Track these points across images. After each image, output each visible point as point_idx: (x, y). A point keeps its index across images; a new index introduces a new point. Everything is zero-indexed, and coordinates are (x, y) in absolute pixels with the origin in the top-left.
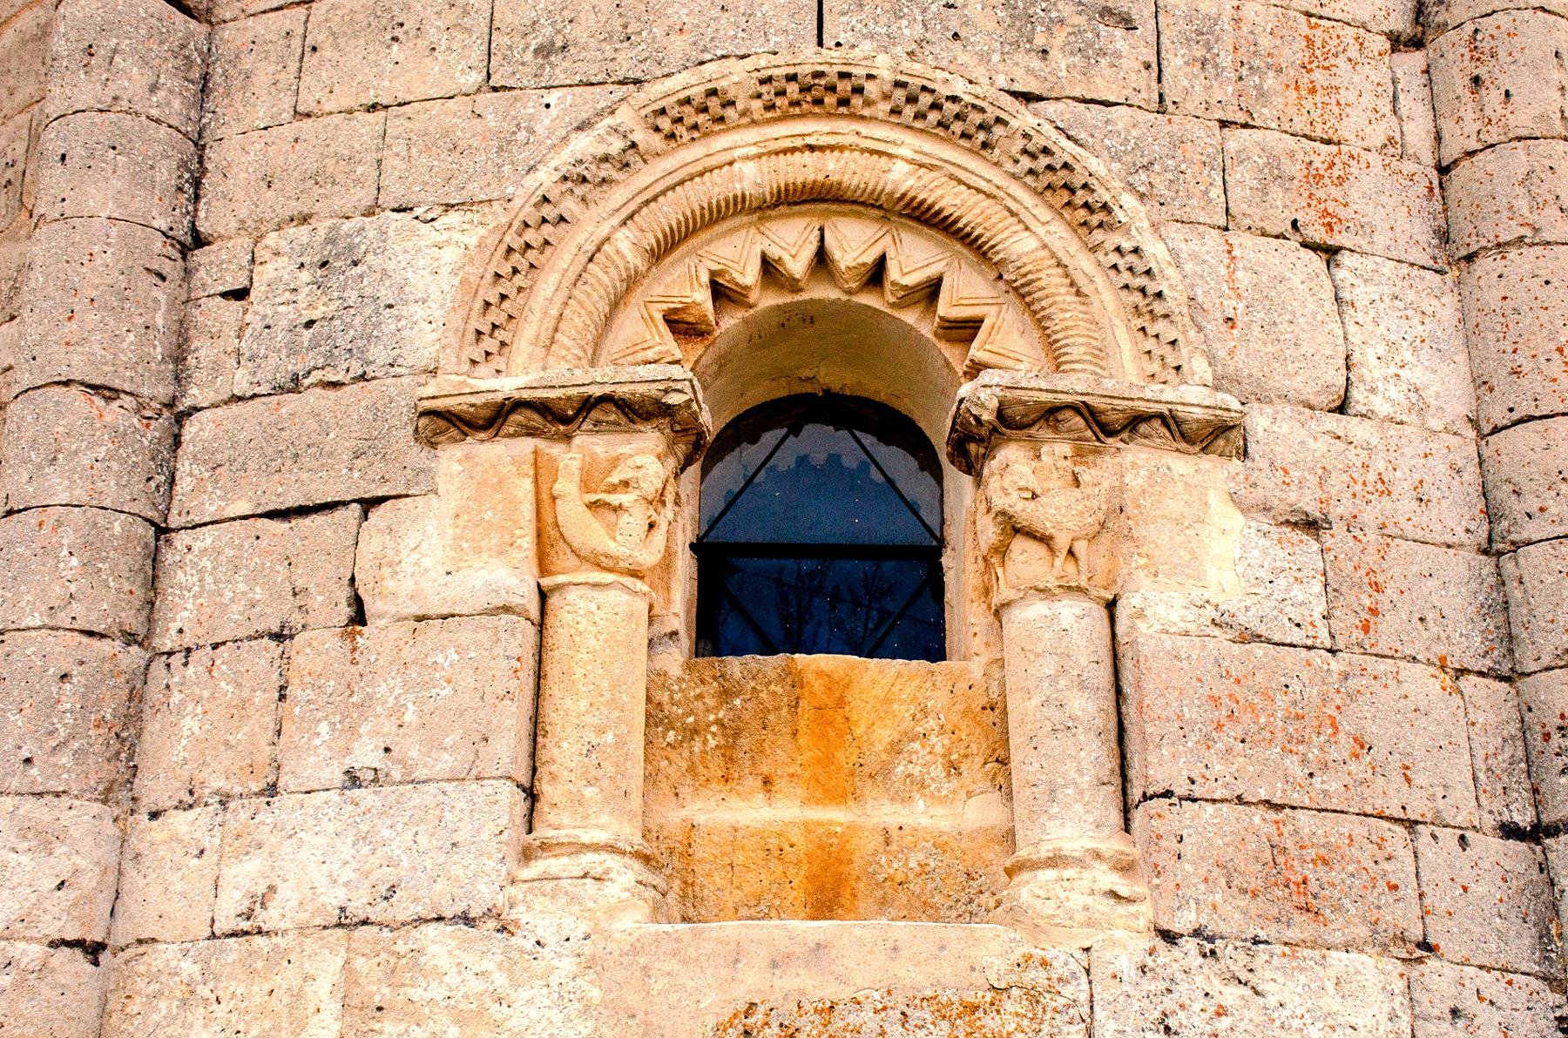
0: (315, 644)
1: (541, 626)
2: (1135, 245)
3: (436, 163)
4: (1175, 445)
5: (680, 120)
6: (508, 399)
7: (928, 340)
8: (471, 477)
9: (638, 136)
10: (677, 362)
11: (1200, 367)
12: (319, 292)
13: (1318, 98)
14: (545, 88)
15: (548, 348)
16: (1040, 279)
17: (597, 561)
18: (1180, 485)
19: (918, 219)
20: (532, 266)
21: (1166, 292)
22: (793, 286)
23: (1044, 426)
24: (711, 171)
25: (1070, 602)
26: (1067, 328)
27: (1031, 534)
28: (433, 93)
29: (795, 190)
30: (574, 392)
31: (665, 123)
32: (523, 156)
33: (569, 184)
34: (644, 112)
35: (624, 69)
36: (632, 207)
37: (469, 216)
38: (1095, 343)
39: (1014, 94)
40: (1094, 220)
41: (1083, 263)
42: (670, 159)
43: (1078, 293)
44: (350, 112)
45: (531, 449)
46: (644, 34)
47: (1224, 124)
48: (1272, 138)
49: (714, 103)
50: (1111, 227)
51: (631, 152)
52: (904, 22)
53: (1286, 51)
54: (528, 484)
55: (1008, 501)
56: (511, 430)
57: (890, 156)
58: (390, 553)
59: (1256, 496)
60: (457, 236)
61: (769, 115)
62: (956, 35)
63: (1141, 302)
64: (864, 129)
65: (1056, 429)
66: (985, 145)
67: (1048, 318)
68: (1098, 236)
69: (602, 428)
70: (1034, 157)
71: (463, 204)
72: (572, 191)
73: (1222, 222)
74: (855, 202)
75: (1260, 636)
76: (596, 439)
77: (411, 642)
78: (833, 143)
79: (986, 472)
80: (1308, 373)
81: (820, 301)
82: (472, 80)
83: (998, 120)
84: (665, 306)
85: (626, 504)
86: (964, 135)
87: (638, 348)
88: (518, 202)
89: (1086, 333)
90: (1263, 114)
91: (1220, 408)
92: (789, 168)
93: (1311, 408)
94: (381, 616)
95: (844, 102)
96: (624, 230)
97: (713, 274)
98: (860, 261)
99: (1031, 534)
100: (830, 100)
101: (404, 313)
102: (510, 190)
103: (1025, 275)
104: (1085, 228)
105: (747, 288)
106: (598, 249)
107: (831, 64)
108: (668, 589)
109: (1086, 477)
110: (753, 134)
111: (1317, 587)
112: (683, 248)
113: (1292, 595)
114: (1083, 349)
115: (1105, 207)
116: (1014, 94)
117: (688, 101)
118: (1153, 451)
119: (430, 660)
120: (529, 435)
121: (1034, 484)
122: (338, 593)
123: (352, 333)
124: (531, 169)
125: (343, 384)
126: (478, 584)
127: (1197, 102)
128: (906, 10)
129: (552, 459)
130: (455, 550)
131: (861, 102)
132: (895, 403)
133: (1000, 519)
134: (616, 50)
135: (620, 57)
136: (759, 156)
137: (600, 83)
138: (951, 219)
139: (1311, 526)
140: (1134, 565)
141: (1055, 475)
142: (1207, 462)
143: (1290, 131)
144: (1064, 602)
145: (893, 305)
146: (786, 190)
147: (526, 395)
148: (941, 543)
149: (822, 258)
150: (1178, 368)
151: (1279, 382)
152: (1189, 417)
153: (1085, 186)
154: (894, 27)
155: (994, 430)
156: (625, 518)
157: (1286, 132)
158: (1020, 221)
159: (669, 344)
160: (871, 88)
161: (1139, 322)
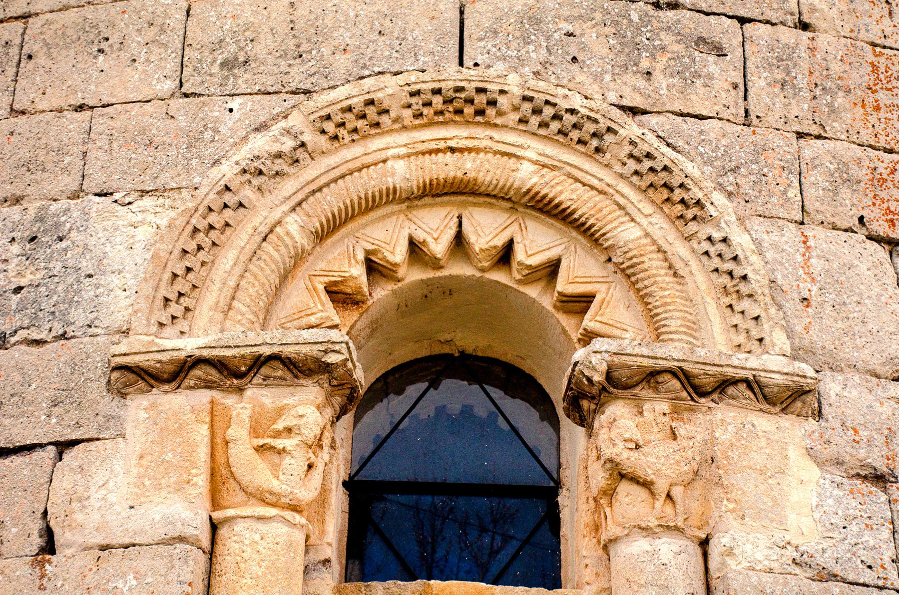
0: (7, 571)
1: (211, 554)
2: (724, 235)
3: (133, 156)
4: (759, 405)
5: (343, 124)
6: (190, 356)
7: (548, 311)
8: (155, 423)
9: (306, 138)
10: (335, 327)
11: (779, 340)
12: (28, 262)
13: (882, 114)
14: (229, 95)
15: (226, 313)
16: (643, 262)
17: (263, 497)
18: (763, 440)
19: (541, 210)
20: (214, 244)
21: (750, 275)
22: (435, 264)
23: (646, 386)
24: (368, 167)
25: (669, 540)
26: (666, 304)
27: (634, 480)
28: (132, 97)
29: (438, 184)
30: (248, 351)
31: (330, 127)
32: (209, 152)
33: (248, 176)
34: (312, 117)
35: (297, 80)
36: (300, 196)
37: (161, 200)
38: (690, 317)
39: (623, 108)
40: (690, 214)
41: (680, 249)
42: (333, 156)
43: (675, 275)
44: (60, 111)
45: (208, 399)
46: (314, 52)
47: (800, 135)
48: (842, 148)
49: (371, 111)
50: (703, 220)
51: (301, 150)
52: (532, 47)
53: (854, 74)
54: (205, 430)
55: (615, 450)
56: (192, 383)
57: (518, 157)
58: (80, 489)
59: (830, 452)
60: (150, 218)
61: (417, 122)
62: (574, 59)
63: (729, 284)
64: (497, 135)
65: (656, 390)
66: (598, 150)
67: (649, 295)
68: (693, 227)
69: (270, 382)
70: (639, 160)
71: (156, 190)
72: (250, 182)
73: (798, 217)
74: (488, 195)
75: (835, 576)
76: (264, 391)
77: (95, 569)
78: (470, 145)
79: (596, 424)
80: (874, 347)
81: (458, 276)
82: (166, 87)
83: (609, 130)
84: (326, 279)
85: (289, 448)
86: (580, 141)
87: (303, 314)
88: (203, 190)
89: (681, 308)
90: (835, 127)
91: (798, 375)
92: (434, 166)
93: (878, 376)
94: (69, 546)
95: (480, 112)
96: (293, 215)
97: (368, 252)
98: (491, 244)
99: (634, 480)
100: (469, 110)
101: (102, 282)
102: (197, 180)
103: (631, 259)
104: (682, 220)
105: (396, 265)
106: (271, 231)
107: (470, 81)
108: (323, 522)
109: (681, 431)
110: (404, 138)
111: (886, 534)
112: (343, 231)
113: (864, 539)
114: (679, 322)
115: (698, 203)
116: (623, 108)
117: (349, 109)
118: (740, 410)
119: (111, 585)
120: (206, 387)
121: (637, 436)
122: (32, 526)
123: (55, 298)
124: (216, 162)
125: (46, 342)
126: (157, 517)
127: (777, 117)
128: (533, 37)
129: (226, 408)
130: (138, 487)
131: (494, 113)
132: (518, 363)
133: (608, 466)
134: (290, 65)
135: (294, 71)
136: (409, 156)
137: (276, 93)
138: (569, 211)
139: (879, 479)
140: (723, 508)
141: (656, 429)
142: (787, 421)
143: (857, 141)
144: (664, 539)
145: (519, 282)
146: (430, 184)
147: (206, 353)
148: (558, 484)
149: (459, 241)
150: (761, 340)
151: (848, 353)
152: (771, 382)
153: (681, 186)
154: (523, 52)
155: (604, 389)
156: (288, 460)
157: (854, 143)
158: (627, 214)
159: (329, 311)
160: (502, 100)
161: (727, 300)
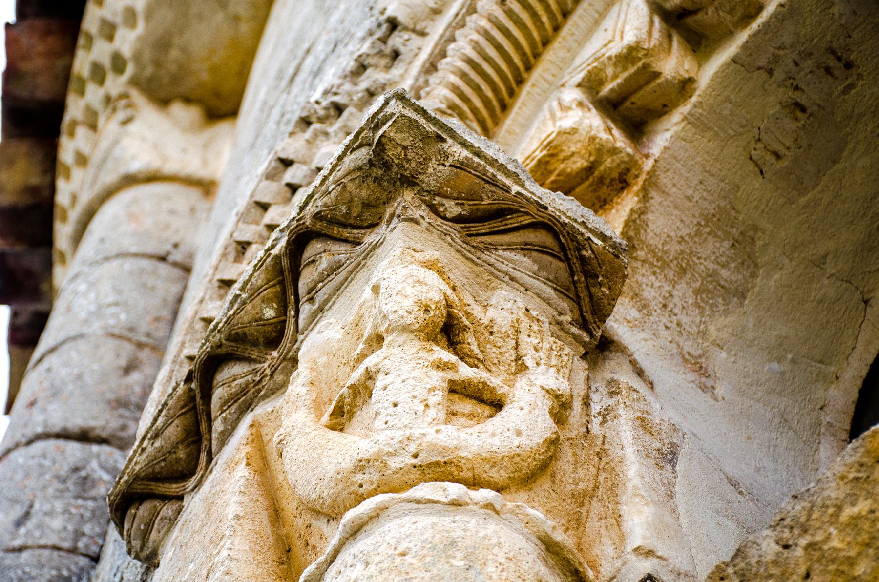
33: (316, 126)
